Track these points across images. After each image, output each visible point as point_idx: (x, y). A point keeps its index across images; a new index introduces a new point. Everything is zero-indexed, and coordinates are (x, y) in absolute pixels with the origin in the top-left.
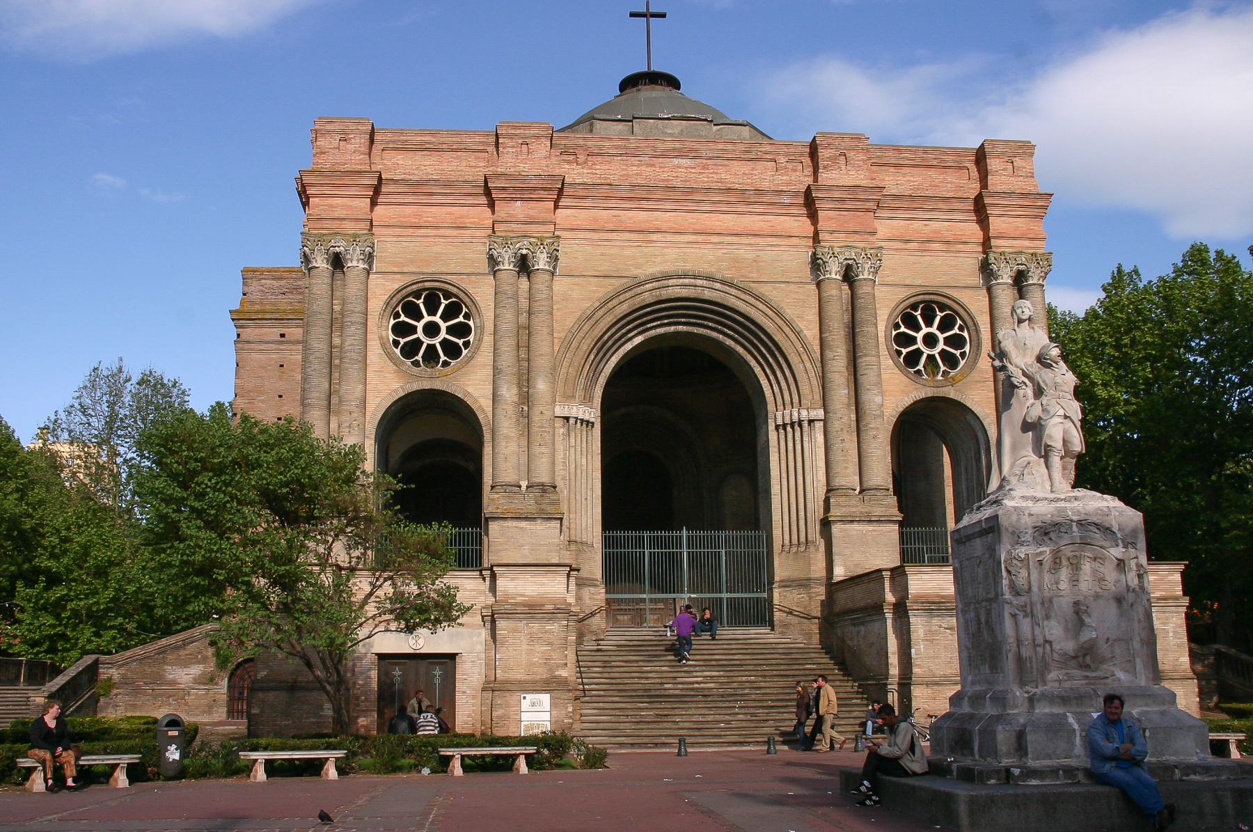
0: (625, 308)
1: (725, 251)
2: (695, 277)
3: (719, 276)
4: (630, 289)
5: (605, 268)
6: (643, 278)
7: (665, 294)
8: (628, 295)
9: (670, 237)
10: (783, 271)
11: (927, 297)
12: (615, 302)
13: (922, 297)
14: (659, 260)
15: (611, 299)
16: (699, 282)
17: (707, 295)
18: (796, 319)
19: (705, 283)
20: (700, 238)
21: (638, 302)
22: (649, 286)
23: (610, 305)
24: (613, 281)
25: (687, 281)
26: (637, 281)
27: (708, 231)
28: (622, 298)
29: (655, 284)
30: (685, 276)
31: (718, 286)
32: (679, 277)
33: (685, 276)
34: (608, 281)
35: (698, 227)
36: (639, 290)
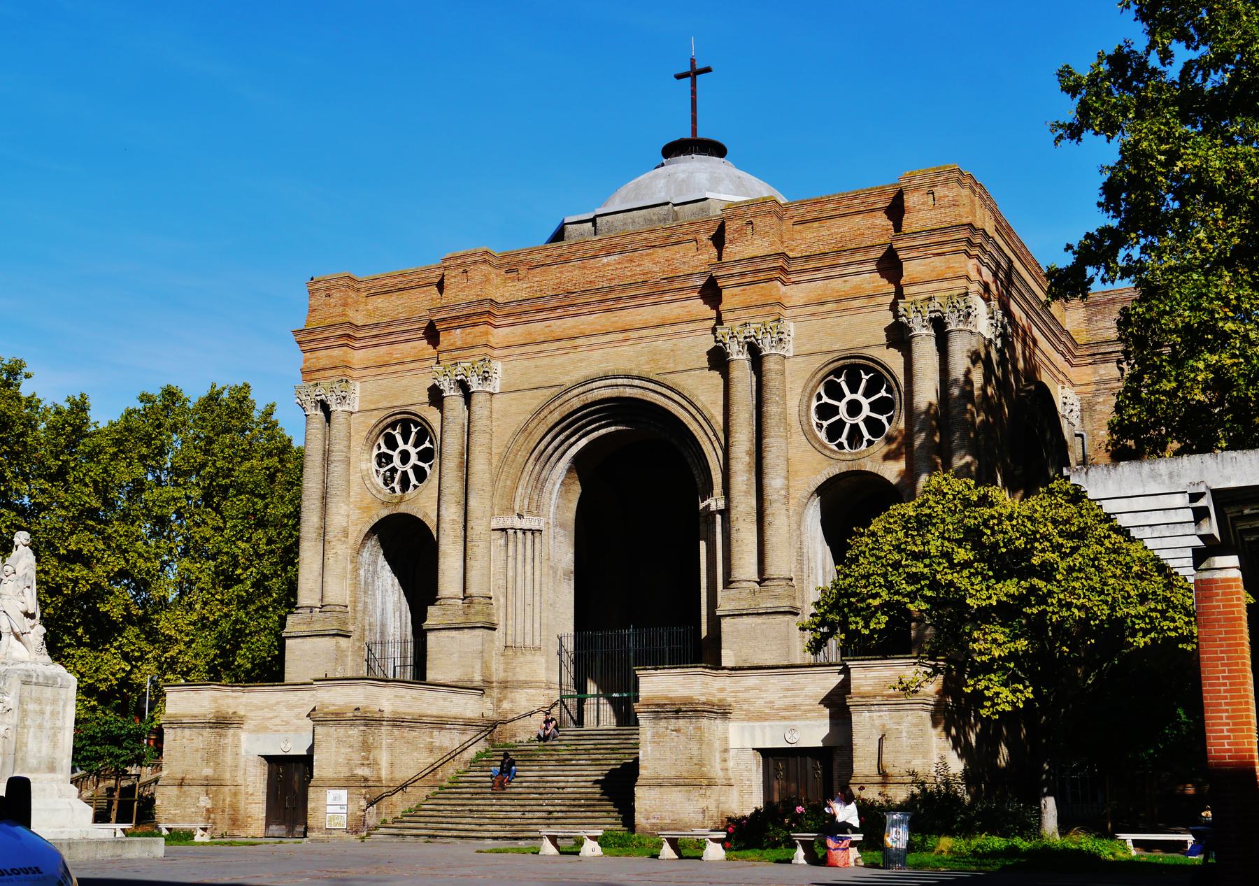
0: (556, 416)
1: (644, 345)
2: (615, 377)
3: (635, 373)
4: (558, 397)
5: (538, 380)
6: (569, 385)
7: (591, 397)
8: (557, 403)
9: (594, 340)
10: (698, 357)
11: (848, 361)
12: (546, 412)
13: (841, 362)
14: (584, 364)
15: (542, 409)
16: (620, 381)
17: (629, 392)
18: (709, 406)
19: (625, 381)
20: (620, 336)
21: (566, 409)
22: (576, 392)
23: (542, 416)
24: (544, 391)
25: (609, 382)
26: (563, 388)
27: (627, 327)
28: (552, 407)
29: (581, 389)
30: (606, 377)
31: (636, 382)
32: (600, 379)
33: (606, 377)
34: (540, 392)
35: (620, 325)
36: (566, 397)
